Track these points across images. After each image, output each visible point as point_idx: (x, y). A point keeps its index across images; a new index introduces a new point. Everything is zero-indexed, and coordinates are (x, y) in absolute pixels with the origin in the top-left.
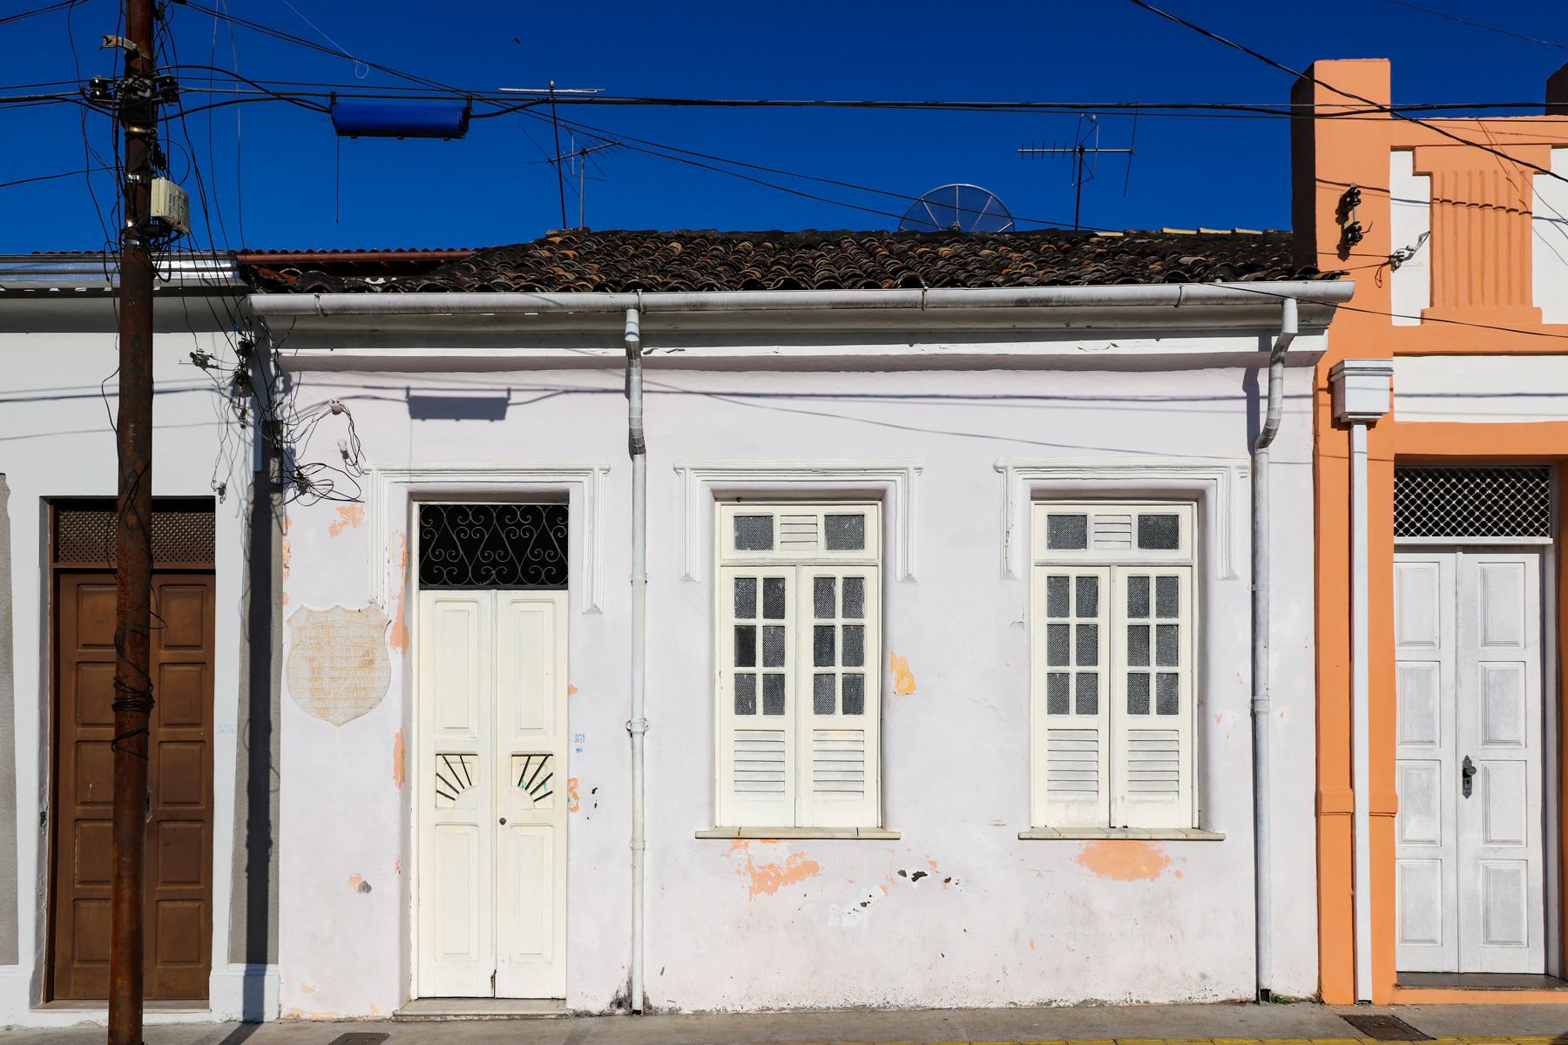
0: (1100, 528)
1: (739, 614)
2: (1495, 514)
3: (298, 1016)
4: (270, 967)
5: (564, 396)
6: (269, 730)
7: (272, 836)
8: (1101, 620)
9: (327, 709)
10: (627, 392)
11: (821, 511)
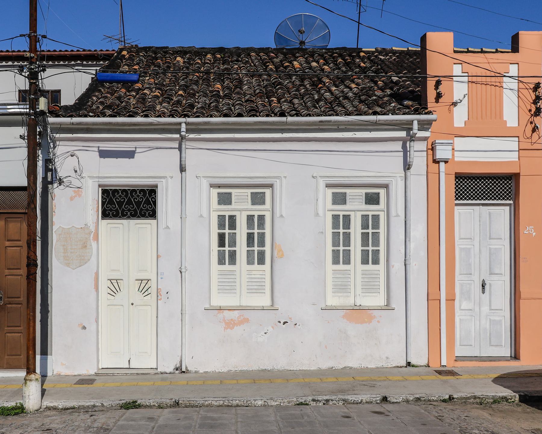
0: (351, 197)
1: (219, 229)
2: (493, 192)
3: (60, 374)
4: (49, 357)
5: (156, 150)
6: (48, 271)
7: (49, 309)
8: (352, 231)
9: (69, 263)
10: (180, 149)
11: (249, 191)
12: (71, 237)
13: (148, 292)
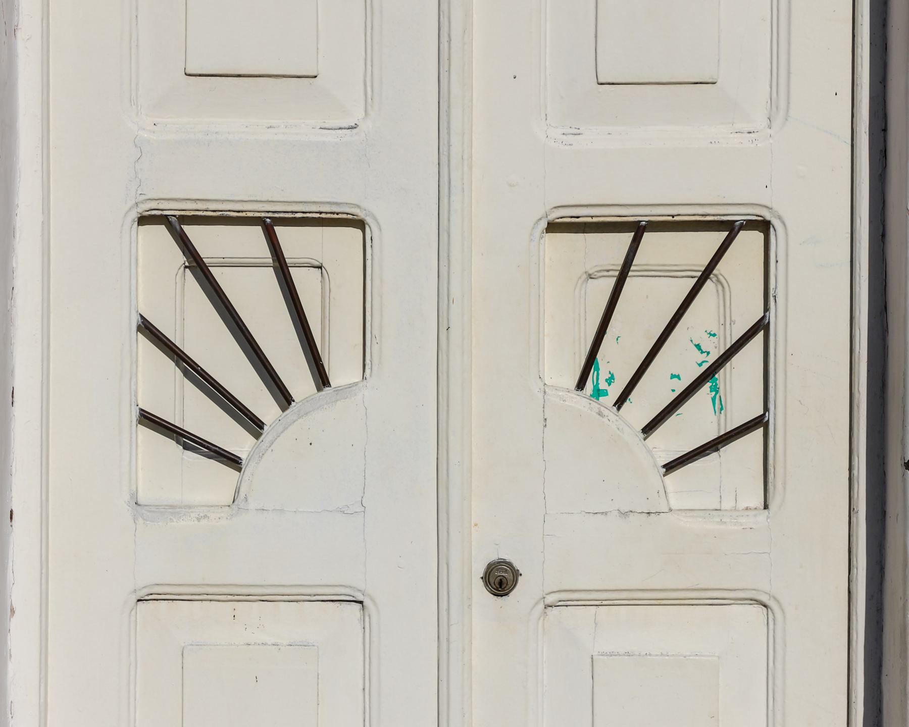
13: (720, 406)
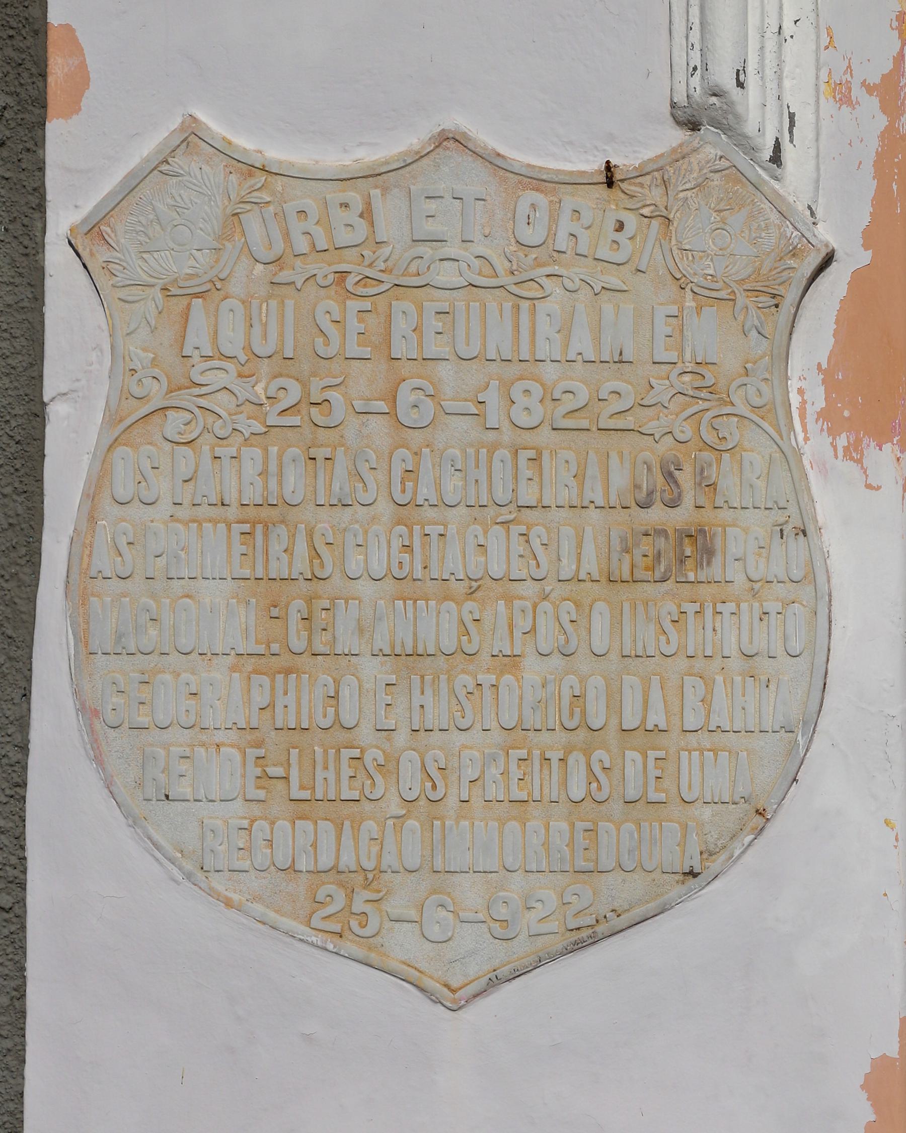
12: (399, 349)
